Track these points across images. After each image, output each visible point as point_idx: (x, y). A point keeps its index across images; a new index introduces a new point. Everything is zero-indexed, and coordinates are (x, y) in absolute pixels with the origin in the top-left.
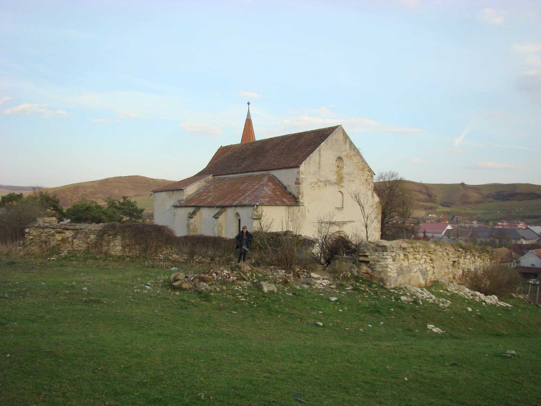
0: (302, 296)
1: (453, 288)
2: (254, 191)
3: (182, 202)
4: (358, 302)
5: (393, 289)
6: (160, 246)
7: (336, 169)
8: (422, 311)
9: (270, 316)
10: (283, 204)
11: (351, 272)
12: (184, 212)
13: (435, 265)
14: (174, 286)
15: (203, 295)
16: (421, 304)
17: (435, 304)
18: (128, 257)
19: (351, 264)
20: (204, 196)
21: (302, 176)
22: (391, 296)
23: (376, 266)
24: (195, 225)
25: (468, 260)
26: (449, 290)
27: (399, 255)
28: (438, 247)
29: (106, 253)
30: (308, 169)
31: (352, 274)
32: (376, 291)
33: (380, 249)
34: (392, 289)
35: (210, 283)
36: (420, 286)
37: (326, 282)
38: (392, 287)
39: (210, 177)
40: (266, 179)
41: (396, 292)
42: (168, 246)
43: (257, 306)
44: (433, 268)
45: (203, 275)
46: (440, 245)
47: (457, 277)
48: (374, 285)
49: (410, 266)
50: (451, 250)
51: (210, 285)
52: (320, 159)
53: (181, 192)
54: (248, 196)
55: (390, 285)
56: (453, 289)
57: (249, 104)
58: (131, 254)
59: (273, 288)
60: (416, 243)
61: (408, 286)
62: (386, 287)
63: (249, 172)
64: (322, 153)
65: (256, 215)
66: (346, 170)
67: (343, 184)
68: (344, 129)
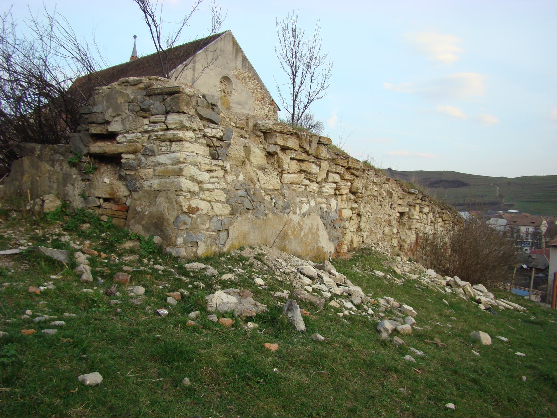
1: (403, 266)
5: (207, 260)
13: (362, 210)
16: (301, 326)
17: (364, 322)
19: (66, 166)
23: (142, 172)
25: (425, 216)
26: (398, 271)
33: (156, 105)
36: (319, 260)
38: (201, 251)
44: (359, 215)
47: (406, 246)
55: (194, 244)
56: (407, 269)
61: (272, 254)
62: (173, 252)
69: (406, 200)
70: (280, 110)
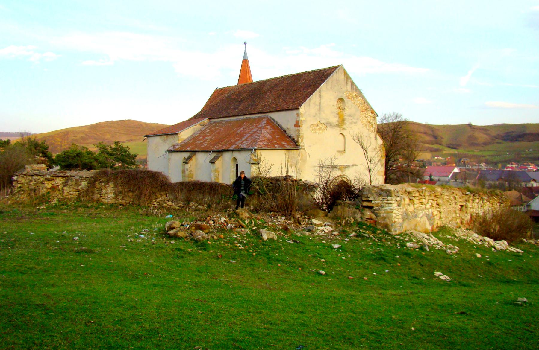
0: (303, 244)
1: (461, 233)
2: (252, 134)
3: (177, 147)
4: (362, 249)
5: (399, 235)
6: (154, 193)
7: (337, 111)
8: (429, 257)
9: (269, 265)
10: (283, 148)
11: (354, 218)
12: (180, 157)
13: (442, 210)
14: (169, 234)
15: (199, 243)
16: (428, 250)
17: (442, 250)
18: (121, 205)
19: (354, 209)
20: (200, 140)
21: (301, 118)
22: (397, 242)
23: (380, 212)
24: (191, 171)
25: (476, 204)
26: (457, 235)
27: (404, 200)
28: (445, 191)
29: (98, 201)
30: (308, 110)
31: (355, 220)
32: (380, 237)
33: (384, 193)
34: (397, 235)
35: (207, 231)
37: (328, 229)
38: (397, 233)
39: (206, 120)
40: (264, 122)
41: (402, 238)
42: (163, 193)
43: (256, 255)
44: (440, 212)
45: (200, 223)
46: (447, 189)
47: (464, 222)
48: (379, 232)
49: (416, 211)
50: (458, 194)
51: (207, 233)
52: (320, 100)
53: (176, 136)
54: (246, 140)
55: (395, 231)
57: (245, 43)
58: (124, 201)
59: (273, 235)
60: (421, 187)
61: (414, 232)
63: (246, 115)
65: (254, 160)
66: (347, 111)
67: (345, 127)
68: (346, 69)
69: (464, 199)
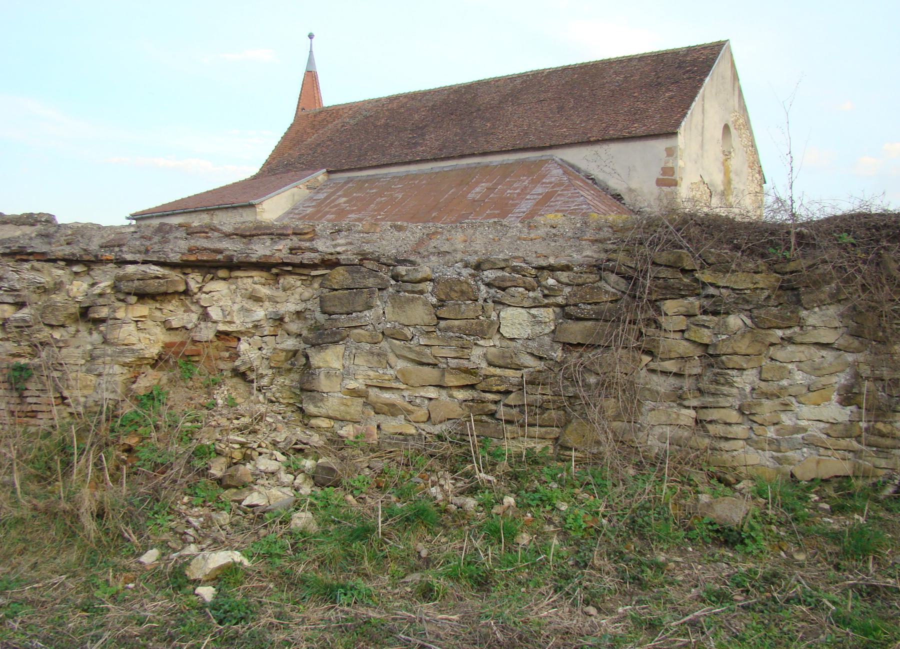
7: (722, 157)
39: (320, 176)
57: (311, 36)
64: (707, 106)
70: (765, 182)
